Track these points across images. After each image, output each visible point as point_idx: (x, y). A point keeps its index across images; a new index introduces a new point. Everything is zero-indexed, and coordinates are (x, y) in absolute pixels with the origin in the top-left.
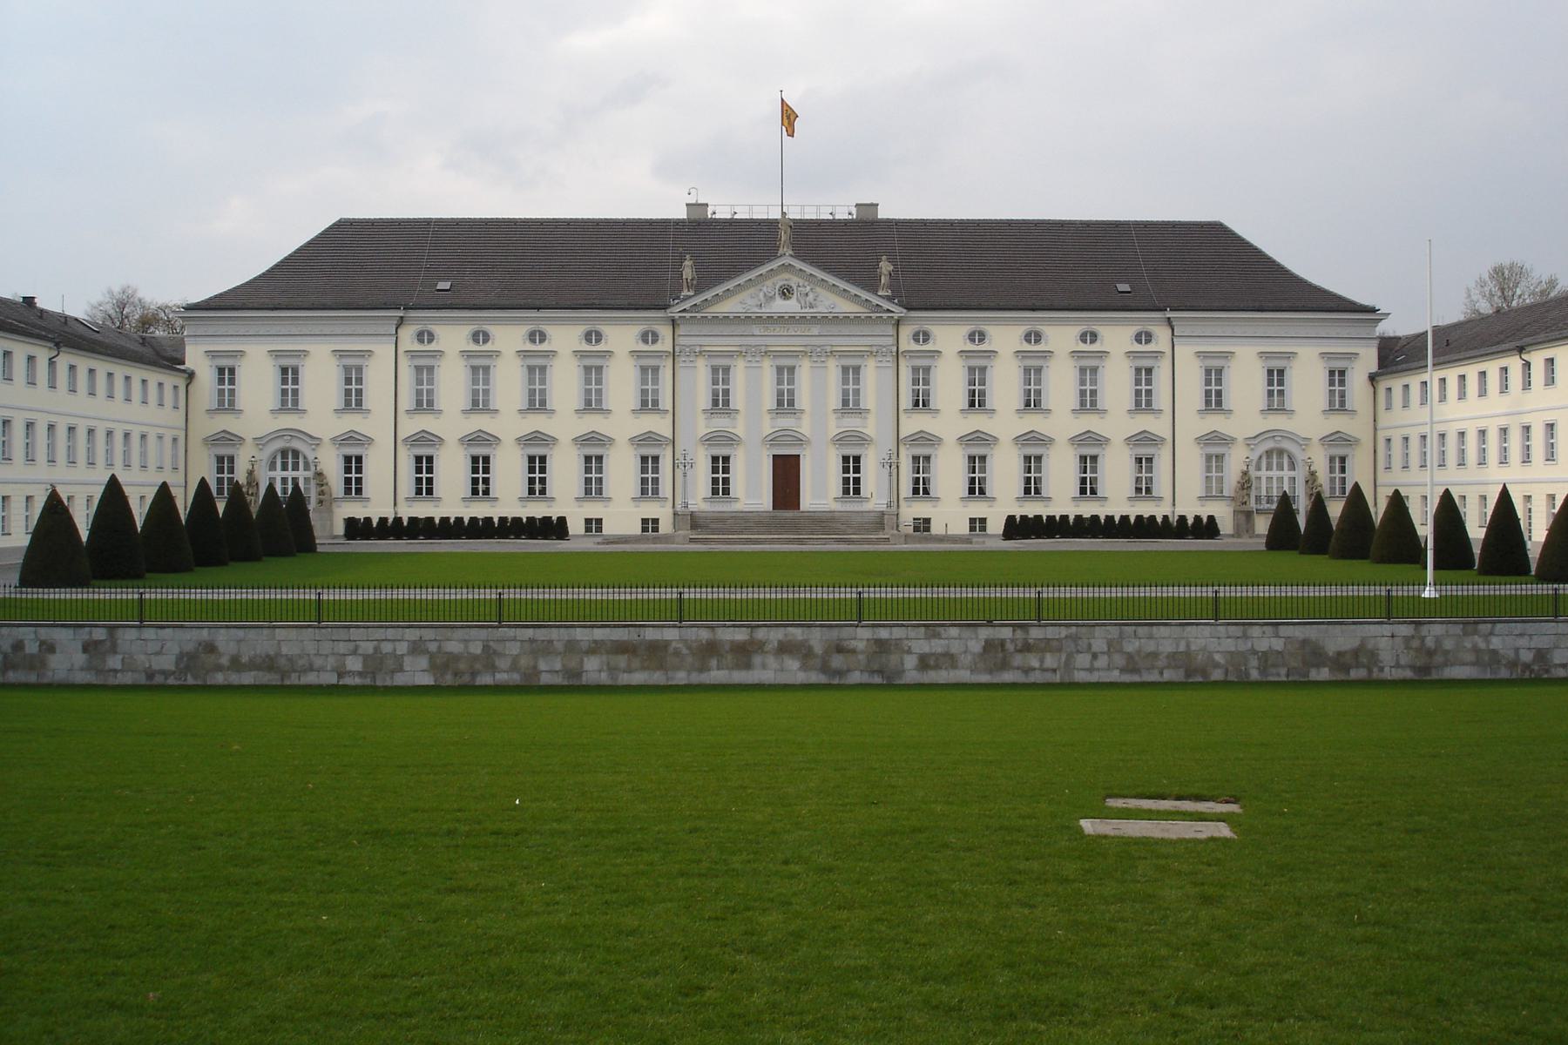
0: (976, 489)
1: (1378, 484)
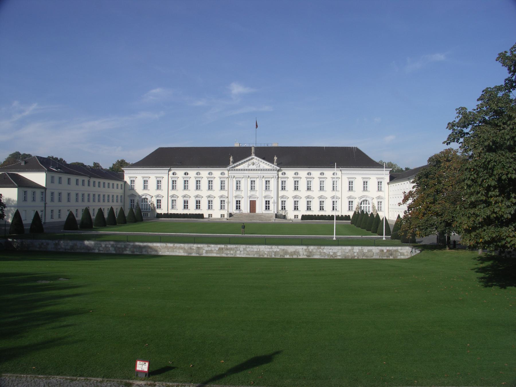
0: (296, 208)
1: (389, 208)
